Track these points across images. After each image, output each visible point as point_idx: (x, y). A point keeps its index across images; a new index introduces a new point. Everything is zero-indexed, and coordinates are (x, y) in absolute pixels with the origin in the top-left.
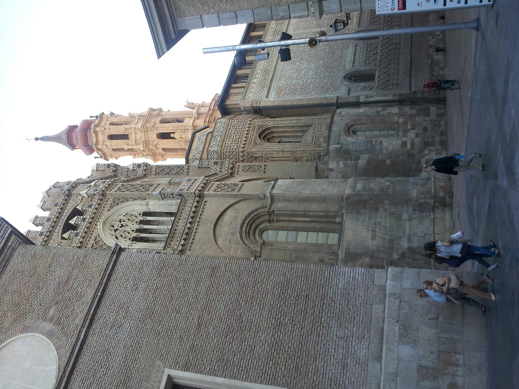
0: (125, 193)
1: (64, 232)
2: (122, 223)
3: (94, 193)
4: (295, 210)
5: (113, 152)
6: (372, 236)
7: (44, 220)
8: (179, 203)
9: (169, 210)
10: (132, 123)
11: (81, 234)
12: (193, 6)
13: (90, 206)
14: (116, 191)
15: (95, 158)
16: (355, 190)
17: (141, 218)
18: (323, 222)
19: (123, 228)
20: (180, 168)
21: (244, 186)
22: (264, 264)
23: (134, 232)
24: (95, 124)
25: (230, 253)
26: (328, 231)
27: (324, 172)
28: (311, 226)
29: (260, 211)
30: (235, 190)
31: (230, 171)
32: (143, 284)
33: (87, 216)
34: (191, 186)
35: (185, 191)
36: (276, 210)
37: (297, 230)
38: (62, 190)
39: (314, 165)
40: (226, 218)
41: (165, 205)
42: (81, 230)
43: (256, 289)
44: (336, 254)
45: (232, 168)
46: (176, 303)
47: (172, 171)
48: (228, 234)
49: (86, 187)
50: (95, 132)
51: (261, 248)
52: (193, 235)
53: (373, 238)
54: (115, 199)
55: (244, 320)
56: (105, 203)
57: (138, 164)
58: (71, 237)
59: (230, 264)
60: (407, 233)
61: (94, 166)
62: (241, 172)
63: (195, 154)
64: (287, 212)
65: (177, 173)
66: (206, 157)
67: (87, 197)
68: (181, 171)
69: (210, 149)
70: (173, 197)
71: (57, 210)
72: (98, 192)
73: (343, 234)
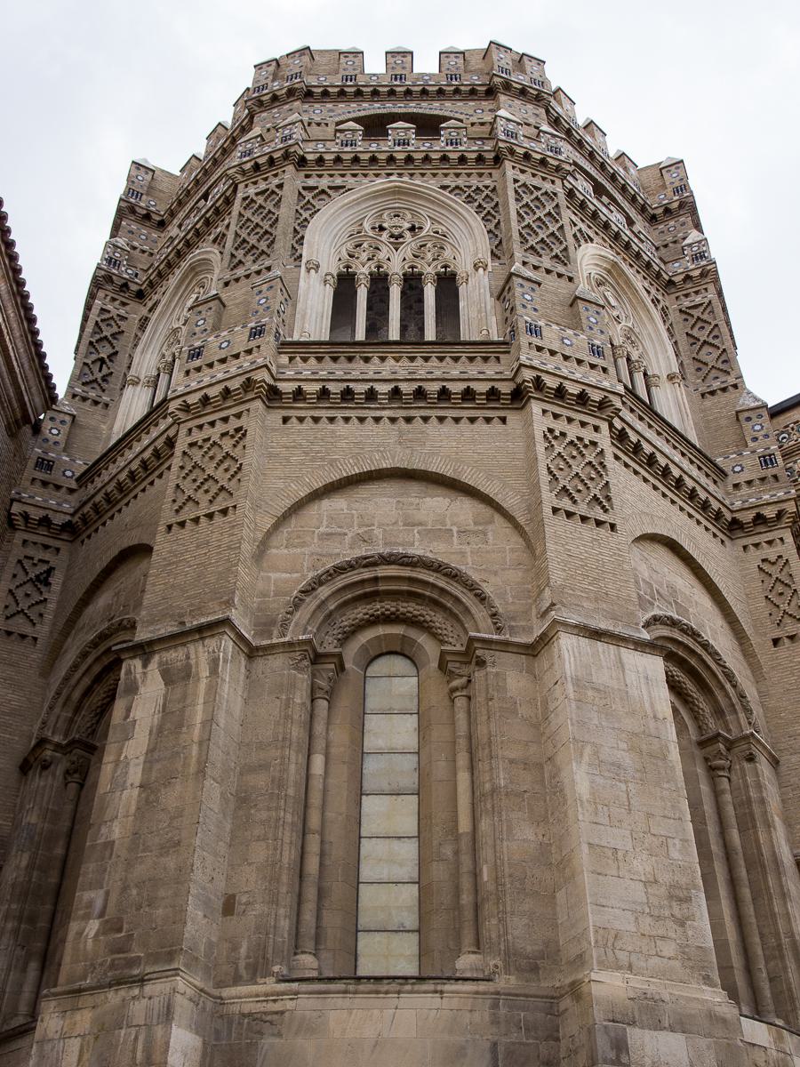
0: (512, 201)
16: (633, 1023)
25: (278, 548)
29: (479, 613)
31: (747, 517)
40: (436, 504)
44: (258, 969)
45: (760, 519)
47: (706, 349)
51: (290, 644)
52: (347, 413)
58: (338, 135)
62: (755, 556)
65: (701, 366)
68: (714, 373)
73: (361, 987)
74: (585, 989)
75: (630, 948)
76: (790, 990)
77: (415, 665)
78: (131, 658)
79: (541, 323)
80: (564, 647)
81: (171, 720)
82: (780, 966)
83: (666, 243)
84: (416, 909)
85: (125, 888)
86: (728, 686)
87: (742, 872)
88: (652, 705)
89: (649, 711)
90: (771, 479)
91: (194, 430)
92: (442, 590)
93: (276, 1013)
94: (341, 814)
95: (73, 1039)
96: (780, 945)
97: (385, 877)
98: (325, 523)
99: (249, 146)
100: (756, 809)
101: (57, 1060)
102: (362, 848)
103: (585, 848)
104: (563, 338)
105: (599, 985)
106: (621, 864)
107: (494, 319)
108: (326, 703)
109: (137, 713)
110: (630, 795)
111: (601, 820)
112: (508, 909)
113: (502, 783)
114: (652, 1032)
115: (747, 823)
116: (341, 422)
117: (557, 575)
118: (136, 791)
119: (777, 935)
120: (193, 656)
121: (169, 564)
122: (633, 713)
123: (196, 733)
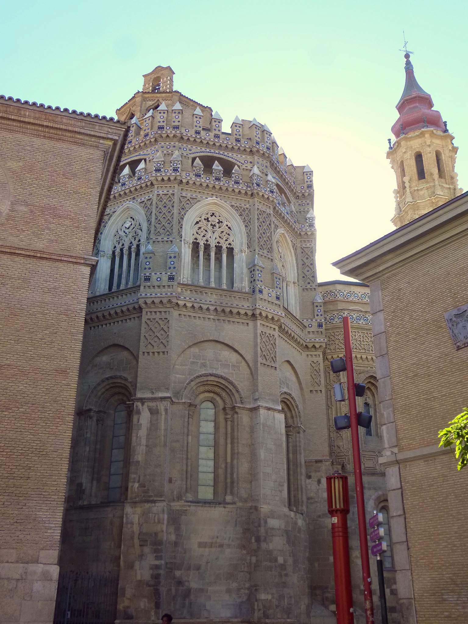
0: (256, 221)
1: (201, 158)
2: (217, 225)
3: (254, 183)
4: (239, 440)
5: (399, 162)
6: (204, 542)
7: (217, 130)
8: (244, 291)
9: (236, 280)
10: (443, 180)
11: (198, 180)
12: (392, 299)
13: (237, 183)
14: (258, 209)
15: (389, 140)
16: (269, 517)
17: (224, 247)
18: (226, 478)
19: (210, 227)
20: (312, 279)
21: (273, 370)
22: (69, 426)
23: (206, 242)
24: (435, 131)
25: (178, 365)
26: (215, 486)
27: (316, 471)
29: (237, 395)
30: (264, 360)
31: (310, 345)
32: (50, 298)
33: (224, 182)
34: (269, 301)
35: (259, 296)
36: (238, 417)
37: (216, 446)
38: (258, 143)
39: (324, 458)
40: (227, 354)
41: (242, 273)
42: (204, 179)
43: (38, 422)
45: (314, 346)
46: (26, 339)
48: (203, 360)
49: (265, 171)
50: (422, 134)
51: (185, 403)
53: (201, 545)
54: (249, 210)
55: (4, 413)
56: (243, 198)
57: (314, 224)
58: (194, 169)
59: (69, 390)
60: (210, 588)
61: (310, 168)
63: (343, 293)
64: (236, 430)
66: (339, 308)
67: (250, 175)
69: (345, 312)
70: (251, 282)
71: (230, 143)
72: (256, 188)
76: (298, 499)
77: (214, 405)
81: (153, 427)
83: (300, 211)
85: (145, 475)
86: (296, 409)
87: (291, 467)
90: (320, 333)
91: (149, 313)
92: (226, 387)
96: (298, 488)
98: (192, 357)
99: (159, 165)
100: (298, 449)
103: (262, 473)
104: (269, 293)
105: (263, 509)
107: (247, 278)
109: (142, 421)
115: (295, 453)
116: (198, 318)
117: (260, 388)
118: (145, 447)
119: (298, 485)
120: (159, 406)
121: (146, 368)
123: (163, 432)
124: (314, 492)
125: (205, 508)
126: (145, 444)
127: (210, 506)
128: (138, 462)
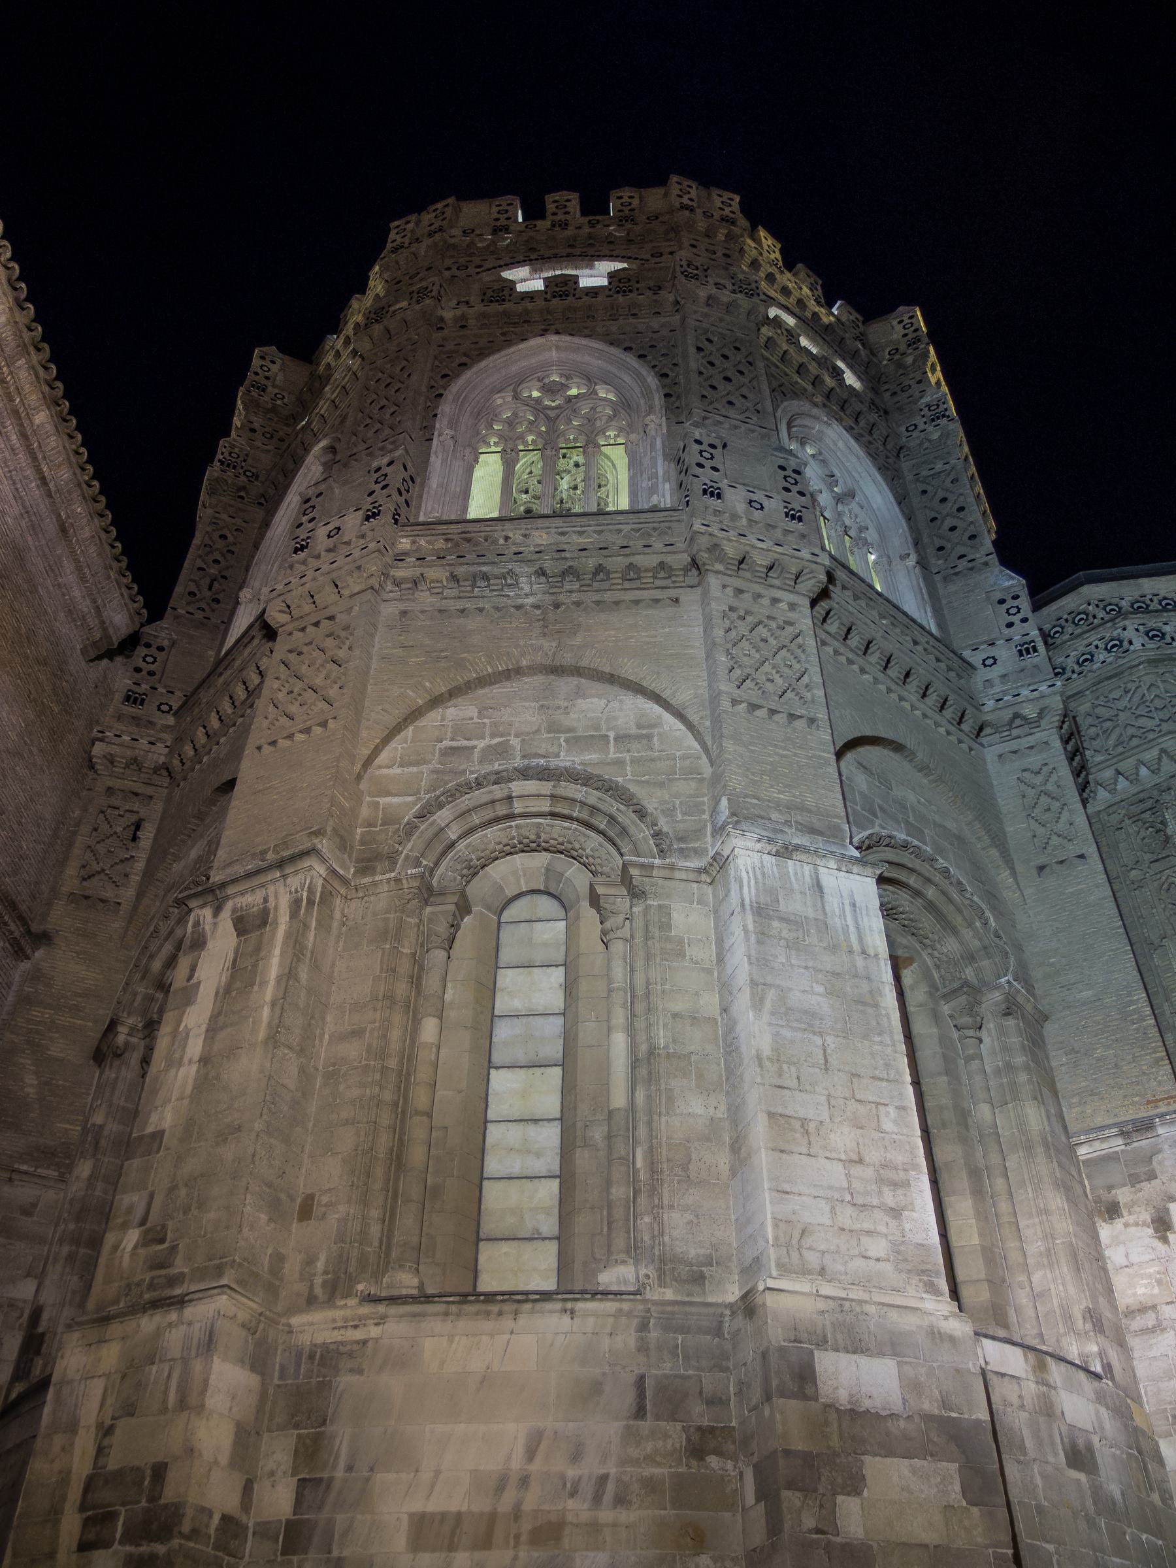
6: (443, 1516)
16: (822, 1343)
26: (563, 1238)
27: (1134, 1180)
28: (580, 1124)
29: (642, 833)
48: (493, 736)
74: (759, 1300)
75: (823, 1247)
78: (201, 907)
79: (724, 484)
80: (742, 867)
82: (1049, 1276)
84: (556, 1210)
85: (173, 1188)
88: (860, 939)
89: (856, 946)
93: (358, 1342)
94: (460, 1092)
95: (96, 1380)
97: (516, 1170)
98: (449, 734)
101: (76, 1405)
102: (488, 1135)
104: (751, 502)
105: (781, 1297)
106: (813, 1138)
107: (667, 486)
108: (443, 954)
109: (201, 973)
110: (829, 1051)
111: (787, 1083)
112: (666, 1202)
113: (662, 1042)
114: (850, 1355)
118: (194, 1068)
120: (272, 900)
122: (834, 949)
123: (269, 993)
124: (1150, 1276)
125: (462, 1324)
126: (196, 1058)
127: (488, 1313)
128: (158, 1135)
